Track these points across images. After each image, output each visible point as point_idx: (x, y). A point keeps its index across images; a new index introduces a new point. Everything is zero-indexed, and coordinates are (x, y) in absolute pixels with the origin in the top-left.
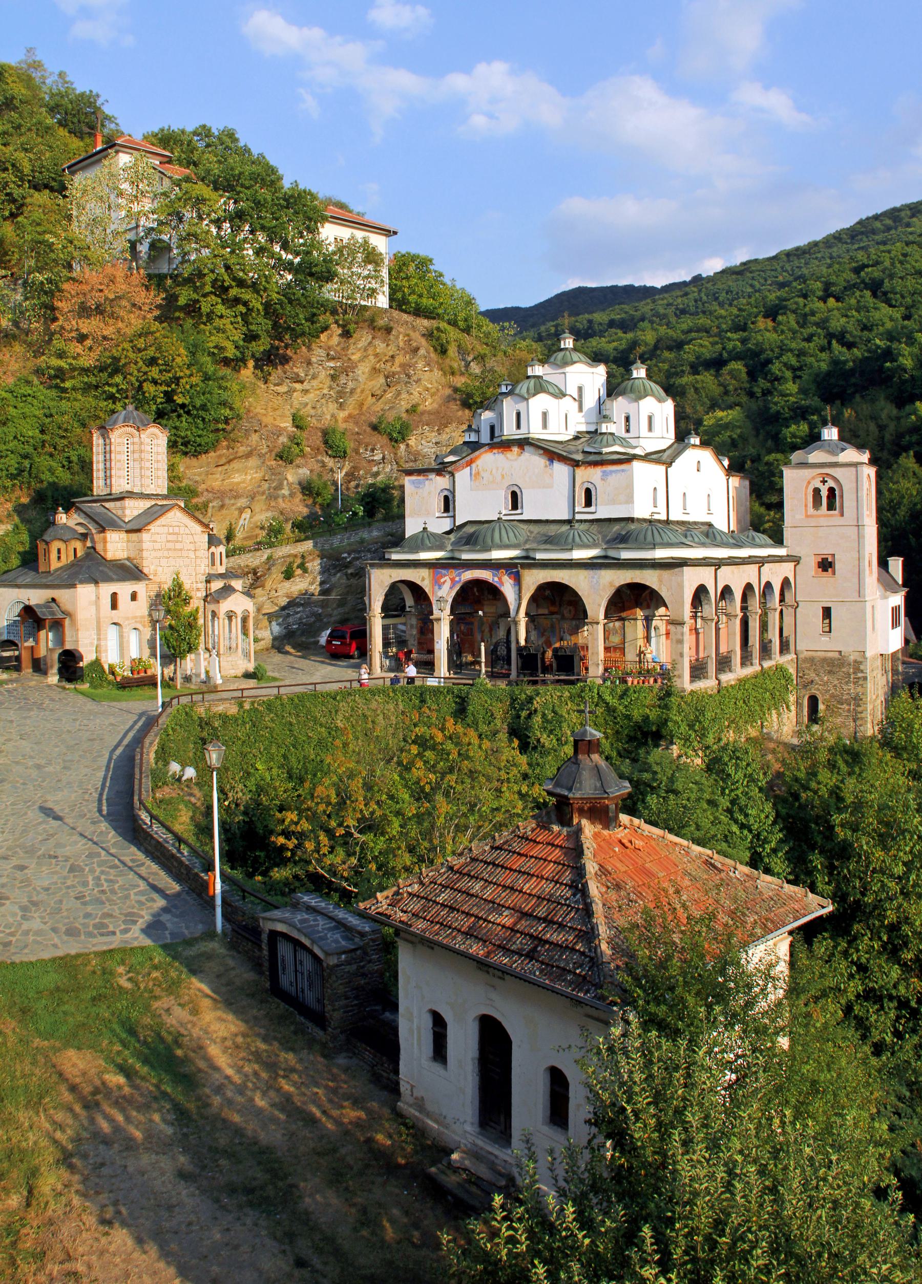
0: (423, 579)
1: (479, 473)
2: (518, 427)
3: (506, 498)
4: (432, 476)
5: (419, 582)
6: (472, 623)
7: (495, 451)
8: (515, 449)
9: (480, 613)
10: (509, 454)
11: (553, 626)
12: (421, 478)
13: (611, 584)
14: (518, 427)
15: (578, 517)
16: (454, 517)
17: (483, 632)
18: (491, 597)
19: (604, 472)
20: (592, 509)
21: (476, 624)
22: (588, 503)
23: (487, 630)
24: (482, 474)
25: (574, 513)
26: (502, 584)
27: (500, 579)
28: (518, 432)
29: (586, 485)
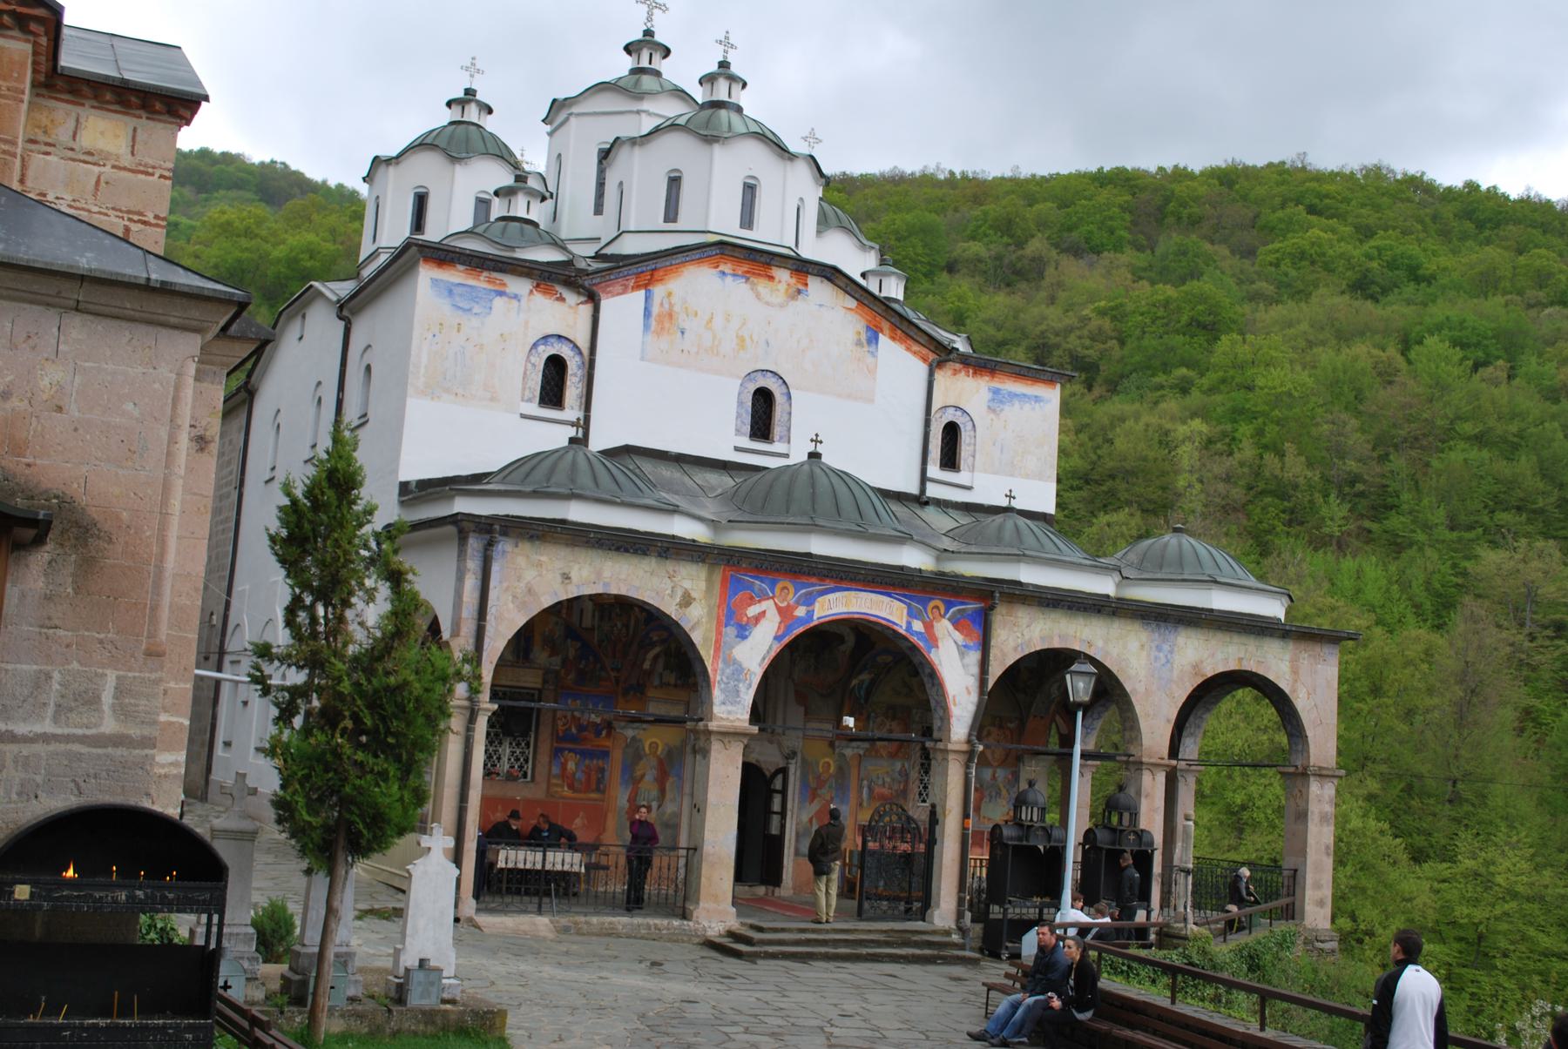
0: (687, 601)
1: (670, 316)
2: (747, 220)
3: (740, 403)
4: (519, 286)
5: (670, 608)
6: (605, 754)
7: (726, 267)
8: (783, 275)
10: (763, 286)
11: (842, 772)
12: (480, 282)
13: (1196, 667)
14: (747, 220)
15: (933, 491)
16: (585, 424)
17: (636, 781)
18: (671, 678)
19: (996, 392)
21: (617, 755)
22: (950, 460)
23: (650, 776)
24: (683, 321)
25: (924, 479)
26: (933, 641)
27: (929, 626)
28: (745, 233)
29: (950, 416)
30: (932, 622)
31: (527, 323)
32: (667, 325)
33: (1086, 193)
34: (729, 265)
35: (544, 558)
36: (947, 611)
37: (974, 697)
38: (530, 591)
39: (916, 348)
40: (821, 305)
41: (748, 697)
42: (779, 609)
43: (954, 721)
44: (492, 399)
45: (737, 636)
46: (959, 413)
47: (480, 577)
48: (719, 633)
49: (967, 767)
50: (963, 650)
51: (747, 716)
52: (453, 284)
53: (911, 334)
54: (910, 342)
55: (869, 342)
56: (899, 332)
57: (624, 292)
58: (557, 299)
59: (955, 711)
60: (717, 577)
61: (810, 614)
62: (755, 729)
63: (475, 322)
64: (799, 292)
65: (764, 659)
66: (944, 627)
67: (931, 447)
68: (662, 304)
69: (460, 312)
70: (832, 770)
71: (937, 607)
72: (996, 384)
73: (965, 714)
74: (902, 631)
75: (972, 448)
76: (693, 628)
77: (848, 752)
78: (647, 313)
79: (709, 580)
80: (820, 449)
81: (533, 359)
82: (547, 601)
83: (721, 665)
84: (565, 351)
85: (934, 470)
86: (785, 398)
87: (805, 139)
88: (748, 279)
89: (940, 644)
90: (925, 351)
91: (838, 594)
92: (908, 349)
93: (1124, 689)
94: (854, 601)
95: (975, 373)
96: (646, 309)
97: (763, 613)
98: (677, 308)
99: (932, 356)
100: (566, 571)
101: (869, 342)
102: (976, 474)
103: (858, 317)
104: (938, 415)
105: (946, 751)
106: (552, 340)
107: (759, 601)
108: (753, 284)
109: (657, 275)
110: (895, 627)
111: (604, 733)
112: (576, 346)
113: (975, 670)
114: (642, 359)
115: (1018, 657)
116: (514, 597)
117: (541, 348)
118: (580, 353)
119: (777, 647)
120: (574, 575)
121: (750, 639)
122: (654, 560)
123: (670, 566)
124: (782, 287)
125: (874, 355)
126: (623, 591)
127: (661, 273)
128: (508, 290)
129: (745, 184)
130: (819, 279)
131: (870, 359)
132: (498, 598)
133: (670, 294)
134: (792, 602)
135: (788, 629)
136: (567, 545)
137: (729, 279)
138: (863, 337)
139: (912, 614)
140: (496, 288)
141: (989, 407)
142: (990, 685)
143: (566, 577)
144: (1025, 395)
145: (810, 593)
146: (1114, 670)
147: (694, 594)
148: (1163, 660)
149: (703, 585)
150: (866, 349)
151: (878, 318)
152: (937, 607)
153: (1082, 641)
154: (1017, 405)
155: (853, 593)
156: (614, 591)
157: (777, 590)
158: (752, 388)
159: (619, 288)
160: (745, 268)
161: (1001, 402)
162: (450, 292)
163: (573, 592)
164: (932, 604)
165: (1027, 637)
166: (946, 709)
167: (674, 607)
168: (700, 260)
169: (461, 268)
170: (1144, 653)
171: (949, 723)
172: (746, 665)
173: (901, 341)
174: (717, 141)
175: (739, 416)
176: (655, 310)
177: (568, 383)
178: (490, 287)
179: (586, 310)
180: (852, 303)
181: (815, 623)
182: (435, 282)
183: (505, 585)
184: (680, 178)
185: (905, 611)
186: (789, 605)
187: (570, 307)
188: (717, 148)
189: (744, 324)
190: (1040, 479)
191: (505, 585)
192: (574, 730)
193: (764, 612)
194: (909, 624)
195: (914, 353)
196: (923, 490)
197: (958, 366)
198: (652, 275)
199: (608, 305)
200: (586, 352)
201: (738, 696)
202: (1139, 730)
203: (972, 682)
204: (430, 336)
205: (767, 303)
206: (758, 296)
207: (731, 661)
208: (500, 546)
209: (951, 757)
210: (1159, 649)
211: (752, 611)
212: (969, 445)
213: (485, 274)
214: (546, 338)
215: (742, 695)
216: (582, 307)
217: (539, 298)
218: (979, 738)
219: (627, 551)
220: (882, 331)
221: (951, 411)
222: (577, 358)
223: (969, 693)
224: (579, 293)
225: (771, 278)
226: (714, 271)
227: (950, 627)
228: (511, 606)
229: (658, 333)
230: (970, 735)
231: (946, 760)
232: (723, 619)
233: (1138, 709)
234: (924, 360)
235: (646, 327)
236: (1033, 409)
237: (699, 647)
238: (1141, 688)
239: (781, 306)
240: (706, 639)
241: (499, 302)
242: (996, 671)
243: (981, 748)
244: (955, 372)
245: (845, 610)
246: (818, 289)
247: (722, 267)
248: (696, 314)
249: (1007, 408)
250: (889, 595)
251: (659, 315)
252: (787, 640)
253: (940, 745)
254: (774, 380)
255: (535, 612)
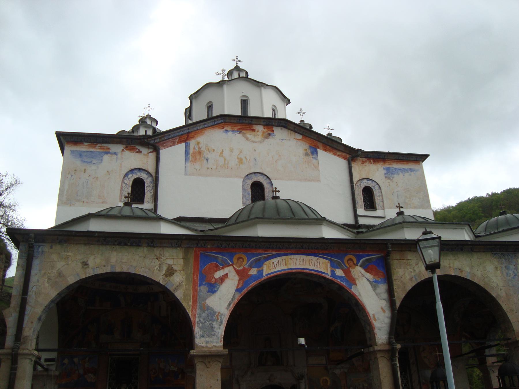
0: (170, 272)
1: (200, 153)
3: (244, 190)
5: (159, 278)
7: (229, 128)
8: (260, 128)
9: (302, 341)
10: (250, 135)
12: (97, 149)
15: (362, 221)
19: (388, 169)
20: (379, 213)
25: (356, 216)
26: (352, 281)
27: (347, 272)
29: (365, 183)
30: (349, 269)
31: (121, 164)
32: (198, 157)
33: (466, 206)
34: (230, 127)
35: (70, 254)
36: (358, 261)
37: (388, 314)
38: (60, 274)
39: (339, 153)
40: (282, 139)
41: (220, 331)
42: (238, 272)
43: (376, 331)
44: (103, 203)
45: (209, 292)
46: (370, 182)
47: (25, 269)
48: (195, 291)
49: (392, 360)
50: (374, 285)
51: (221, 344)
52: (82, 152)
53: (335, 146)
54: (336, 151)
55: (312, 153)
56: (328, 147)
57: (174, 144)
58: (137, 152)
59: (376, 324)
60: (191, 257)
61: (261, 273)
62: (226, 351)
63: (94, 167)
64: (270, 135)
65: (230, 304)
66: (358, 271)
67: (357, 200)
68: (194, 148)
69: (85, 164)
70: (329, 384)
71: (351, 259)
72: (387, 166)
73: (384, 325)
74: (329, 277)
75: (381, 198)
76: (176, 289)
77: (337, 372)
78: (187, 153)
79: (186, 259)
80: (278, 194)
81: (125, 181)
82: (72, 280)
83: (198, 311)
84: (143, 176)
85: (361, 211)
86: (270, 185)
87: (298, 113)
88: (240, 132)
89: (357, 282)
90: (344, 154)
91: (279, 258)
92: (335, 154)
93: (491, 296)
94: (291, 261)
95: (374, 162)
96: (186, 151)
97: (227, 275)
98: (203, 149)
99: (348, 156)
100: (85, 260)
101: (312, 153)
102: (385, 210)
103: (304, 143)
104: (358, 184)
105: (375, 352)
106: (136, 171)
107: (223, 268)
108: (244, 135)
109: (190, 135)
110: (323, 275)
111: (180, 376)
112: (148, 173)
113: (385, 296)
114: (186, 174)
115: (414, 284)
116: (49, 279)
117: (130, 176)
118: (151, 176)
119: (238, 297)
120: (91, 263)
121: (218, 293)
122: (145, 249)
123: (157, 251)
124: (260, 134)
125: (316, 159)
126: (125, 270)
127: (193, 134)
128: (111, 151)
129: (241, 100)
130: (279, 128)
131: (314, 161)
132: (38, 281)
133: (198, 143)
134: (246, 266)
135: (245, 284)
136: (85, 244)
137: (230, 133)
138: (309, 151)
139: (334, 266)
140: (105, 151)
141: (386, 177)
142: (398, 304)
143: (85, 264)
144: (404, 169)
145: (259, 260)
146: (481, 284)
147: (175, 268)
148: (512, 275)
149: (181, 261)
150: (311, 157)
151: (315, 142)
152: (351, 259)
153: (455, 269)
154: (401, 174)
155: (290, 257)
156: (118, 270)
157: (235, 260)
158: (250, 182)
159: (171, 144)
160: (239, 127)
161: (392, 174)
162: (81, 155)
163: (90, 272)
164: (347, 258)
165: (417, 271)
166: (370, 324)
167: (161, 277)
168: (213, 126)
169: (86, 144)
170: (499, 272)
171: (374, 333)
172: (217, 309)
173: (330, 151)
174: (224, 84)
175: (244, 196)
176: (191, 151)
177: (146, 191)
178: (102, 151)
179: (153, 156)
180: (300, 137)
181: (265, 278)
182: (72, 152)
183: (43, 272)
184: (212, 105)
185: (329, 265)
186: (244, 269)
187: (144, 155)
188: (225, 87)
189: (241, 152)
190: (423, 209)
191: (43, 272)
192: (161, 376)
193: (227, 275)
194: (333, 272)
195: (339, 156)
196: (356, 221)
197: (364, 159)
198: (188, 136)
199: (164, 153)
200: (154, 175)
201: (213, 331)
202: (509, 321)
203: (384, 304)
204: (70, 176)
205: (253, 142)
206: (247, 139)
207: (205, 308)
208: (40, 250)
209: (379, 355)
210: (507, 268)
211: (218, 274)
212: (379, 196)
213: (99, 145)
214: (132, 171)
215: (216, 330)
216: (150, 154)
217: (127, 153)
218: (398, 341)
219: (126, 245)
220: (318, 148)
221: (365, 181)
222: (150, 178)
223: (384, 311)
224: (149, 148)
225: (254, 130)
226: (222, 130)
227: (363, 271)
228: (47, 285)
229: (195, 160)
230: (390, 338)
231: (376, 358)
232: (197, 281)
233: (504, 307)
234: (345, 158)
235: (187, 159)
236: (410, 175)
237: (181, 301)
238: (503, 294)
239: (261, 142)
240: (186, 295)
241: (106, 157)
242: (400, 295)
243: (399, 346)
244: (363, 162)
245: (285, 268)
246: (279, 133)
247: (224, 129)
248: (214, 150)
249: (395, 176)
250: (315, 255)
251: (194, 155)
252: (245, 291)
253: (371, 349)
254: (262, 177)
255: (64, 287)
